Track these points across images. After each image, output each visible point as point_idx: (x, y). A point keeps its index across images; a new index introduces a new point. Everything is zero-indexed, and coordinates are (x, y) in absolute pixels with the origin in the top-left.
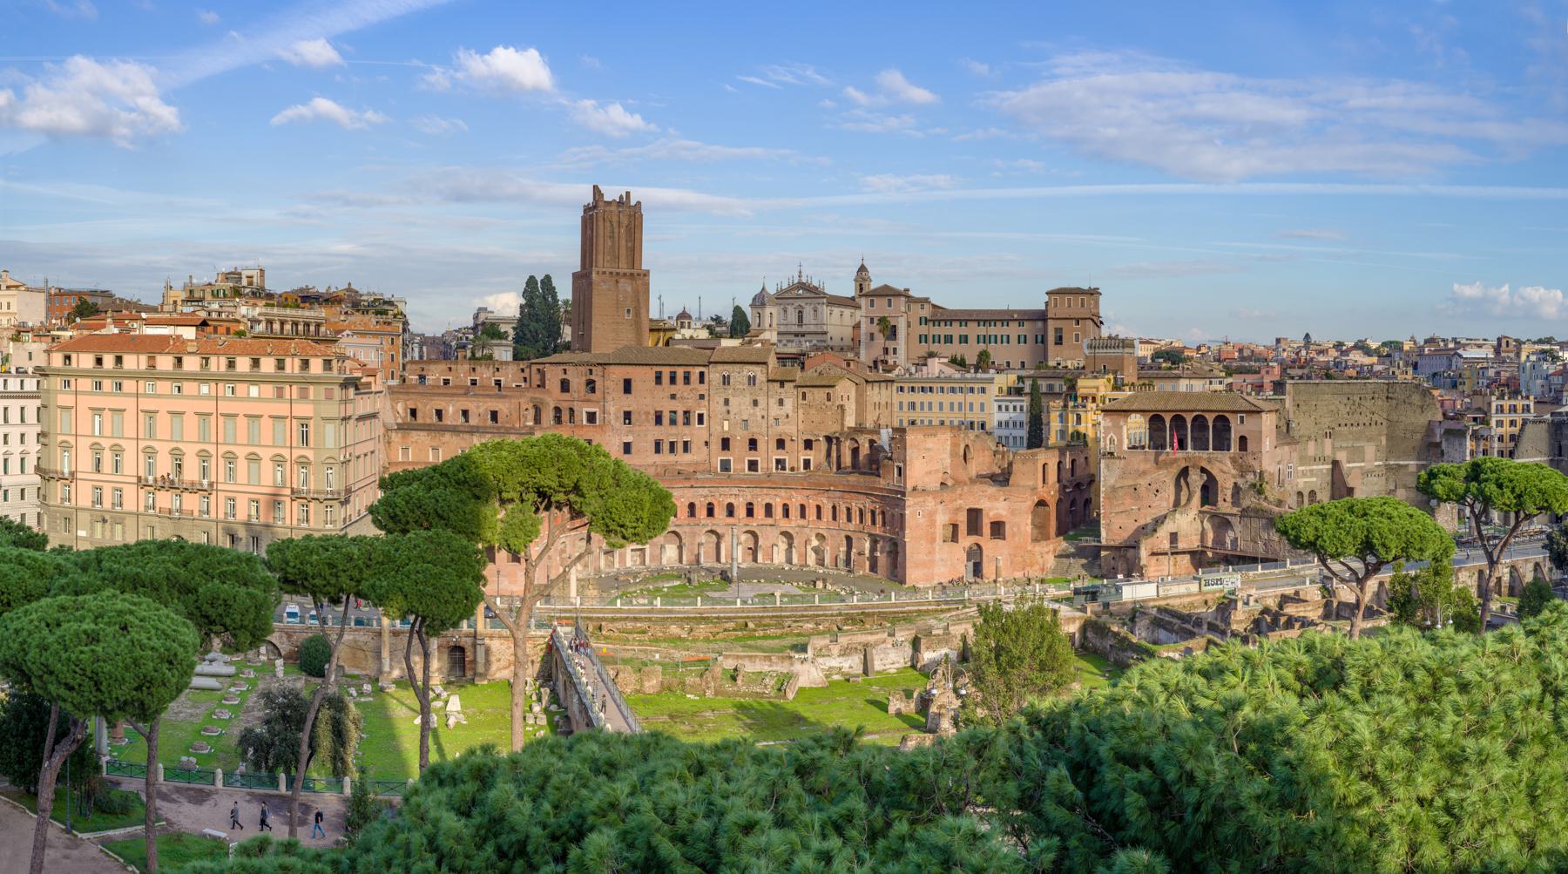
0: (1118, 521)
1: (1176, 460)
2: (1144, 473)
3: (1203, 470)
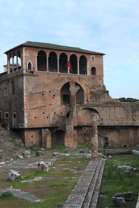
0: (34, 113)
1: (63, 79)
2: (47, 85)
3: (77, 84)
